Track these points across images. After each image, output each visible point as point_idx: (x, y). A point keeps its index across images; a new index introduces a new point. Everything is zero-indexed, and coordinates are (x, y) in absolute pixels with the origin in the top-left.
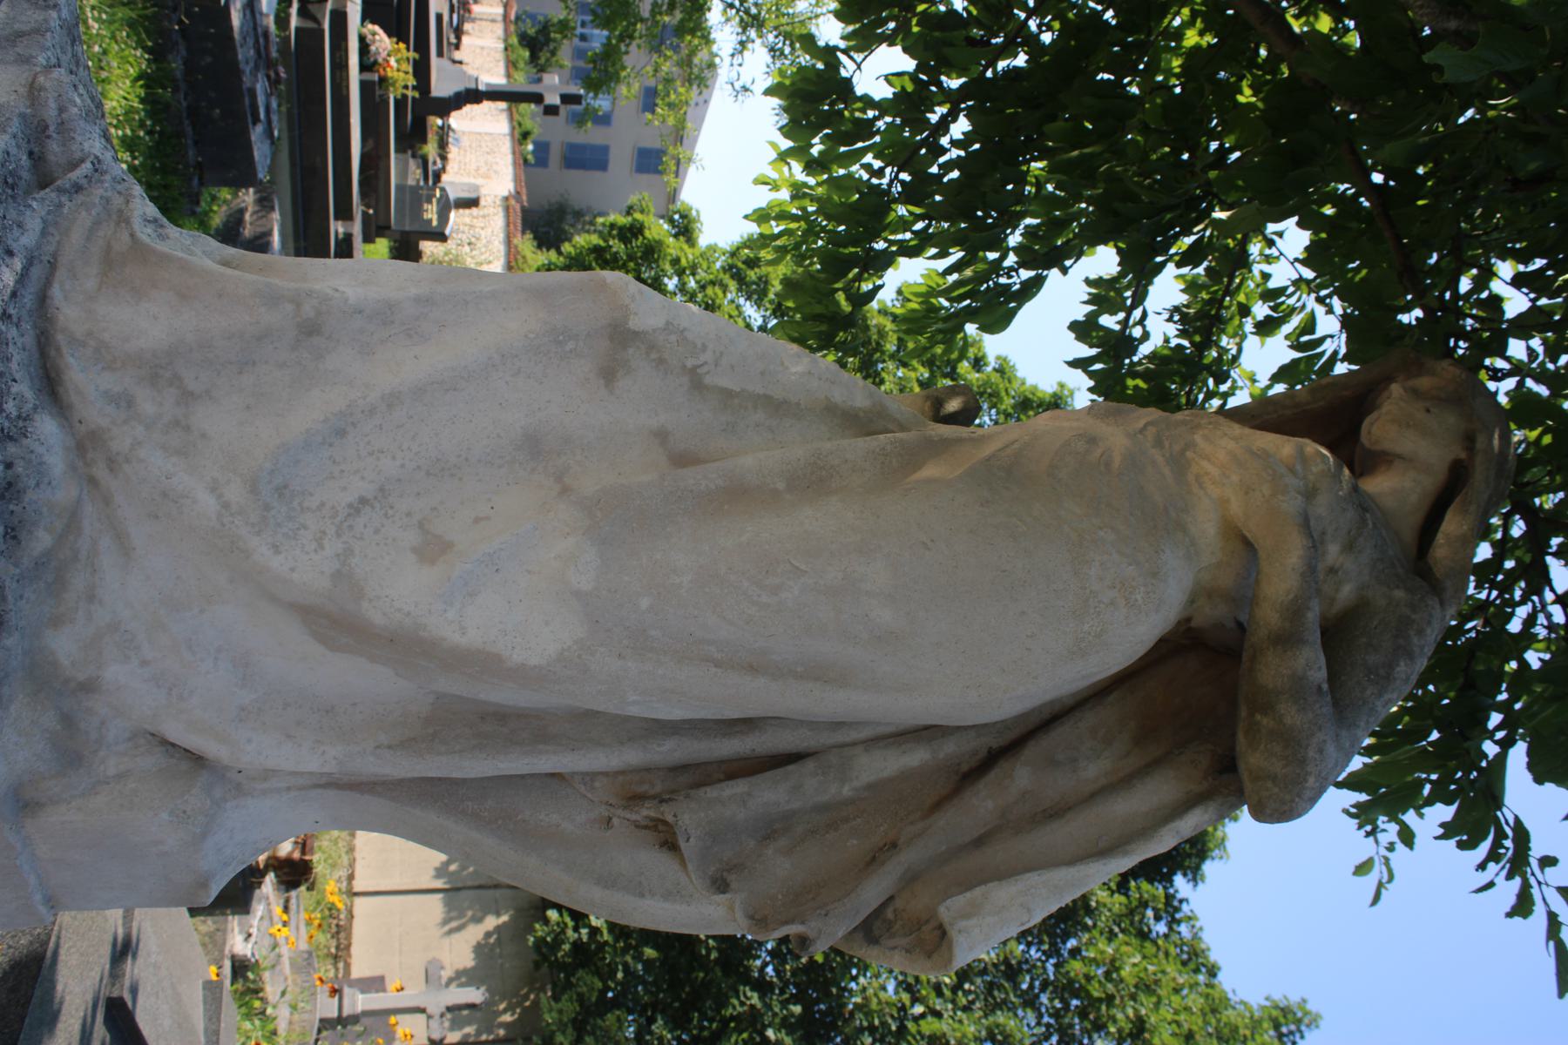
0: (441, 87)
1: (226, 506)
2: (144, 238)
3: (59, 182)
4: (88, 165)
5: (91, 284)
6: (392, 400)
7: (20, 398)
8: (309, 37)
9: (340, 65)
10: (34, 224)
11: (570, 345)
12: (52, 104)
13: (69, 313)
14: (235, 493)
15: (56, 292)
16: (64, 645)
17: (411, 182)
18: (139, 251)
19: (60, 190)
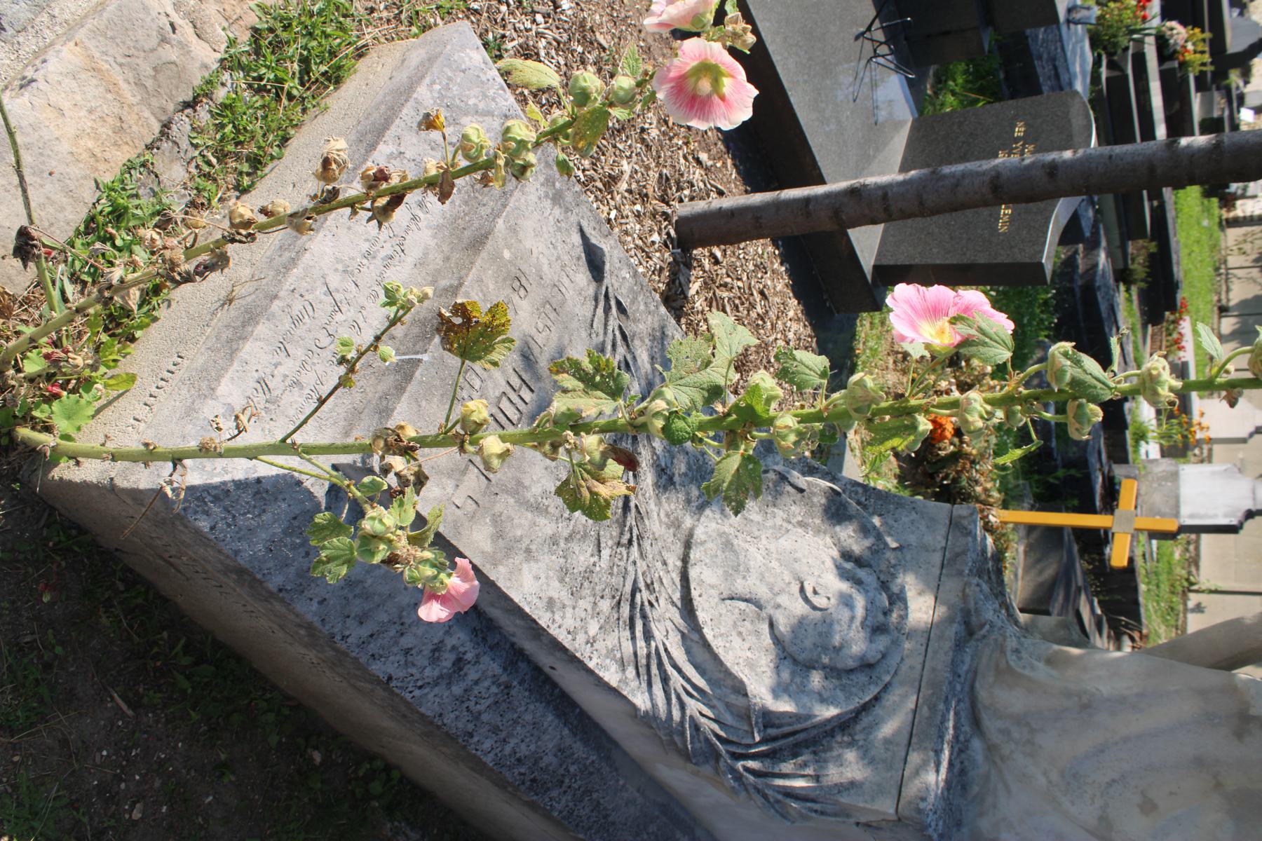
0: (1235, 43)
1: (1050, 782)
2: (1012, 663)
3: (976, 636)
4: (987, 627)
5: (991, 680)
6: (1126, 740)
7: (966, 733)
8: (1117, 83)
9: (1144, 92)
10: (967, 659)
11: (1217, 721)
12: (972, 603)
13: (983, 695)
14: (1054, 776)
15: (977, 685)
16: (985, 824)
17: (1216, 114)
18: (1009, 670)
19: (977, 640)
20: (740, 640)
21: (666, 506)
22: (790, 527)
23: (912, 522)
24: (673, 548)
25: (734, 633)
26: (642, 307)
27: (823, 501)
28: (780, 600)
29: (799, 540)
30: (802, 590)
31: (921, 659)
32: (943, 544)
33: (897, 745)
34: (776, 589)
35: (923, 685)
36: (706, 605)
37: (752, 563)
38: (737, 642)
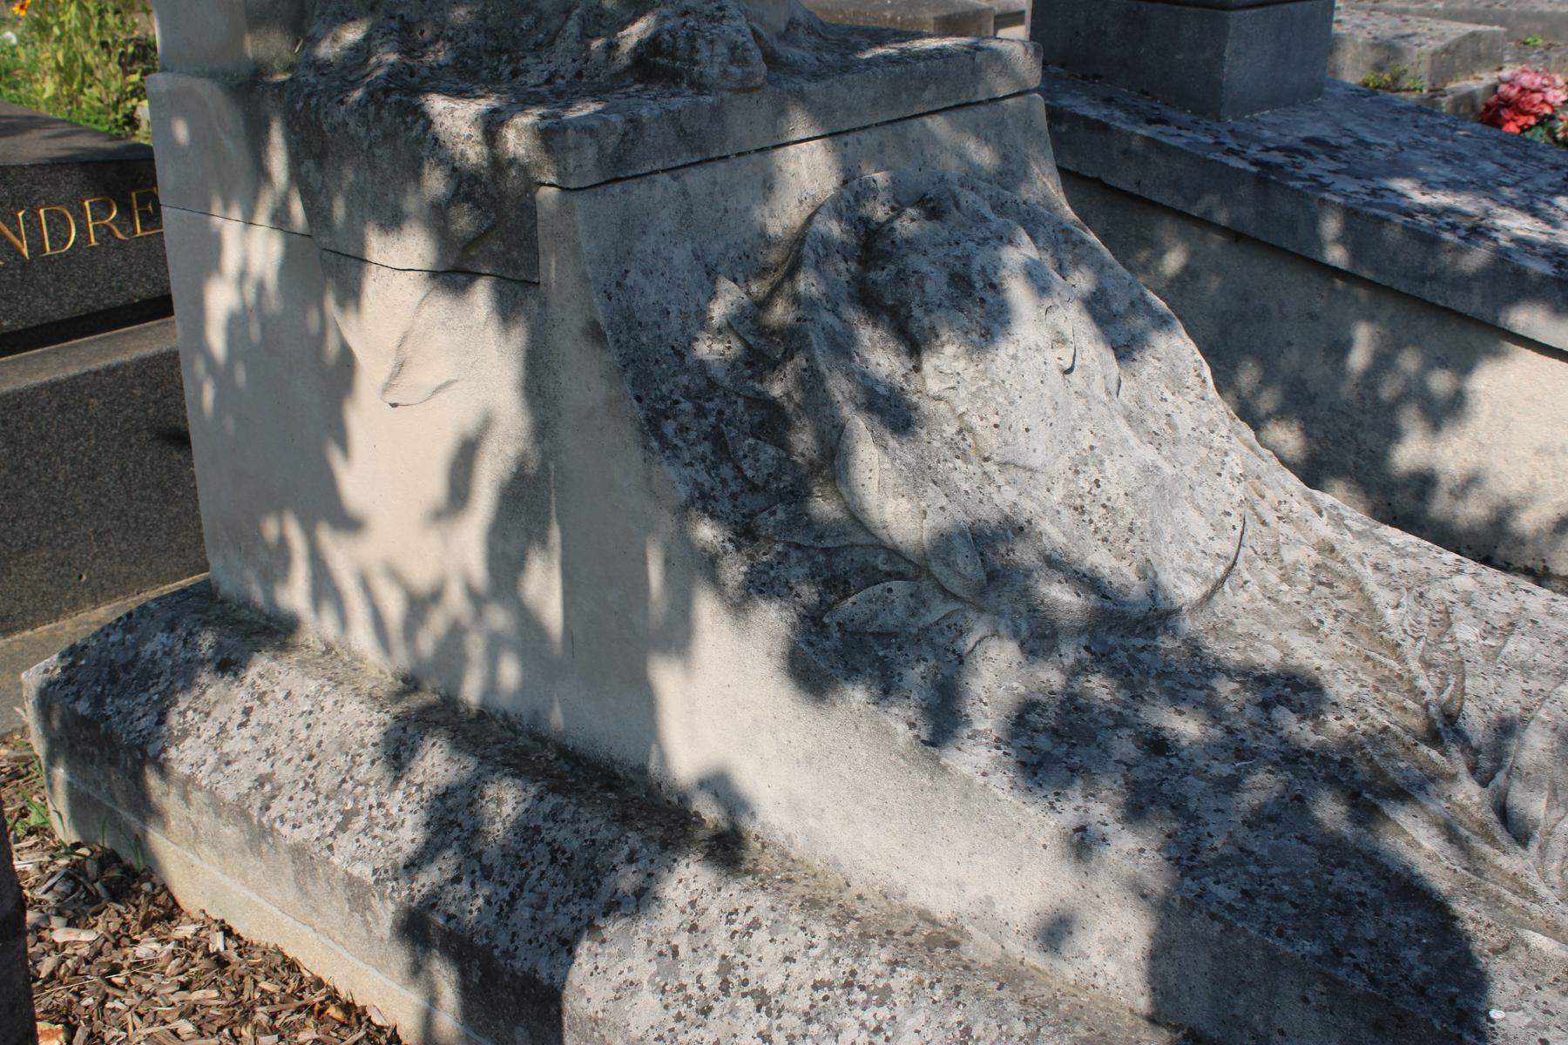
20: (1177, 418)
21: (1258, 659)
22: (991, 467)
23: (647, 273)
24: (1241, 612)
25: (1184, 432)
26: (1412, 955)
27: (892, 443)
28: (1105, 398)
29: (1021, 426)
30: (1071, 370)
31: (864, 135)
32: (664, 178)
33: (977, 125)
34: (1104, 411)
35: (896, 116)
36: (1223, 496)
37: (1132, 470)
38: (1184, 422)
